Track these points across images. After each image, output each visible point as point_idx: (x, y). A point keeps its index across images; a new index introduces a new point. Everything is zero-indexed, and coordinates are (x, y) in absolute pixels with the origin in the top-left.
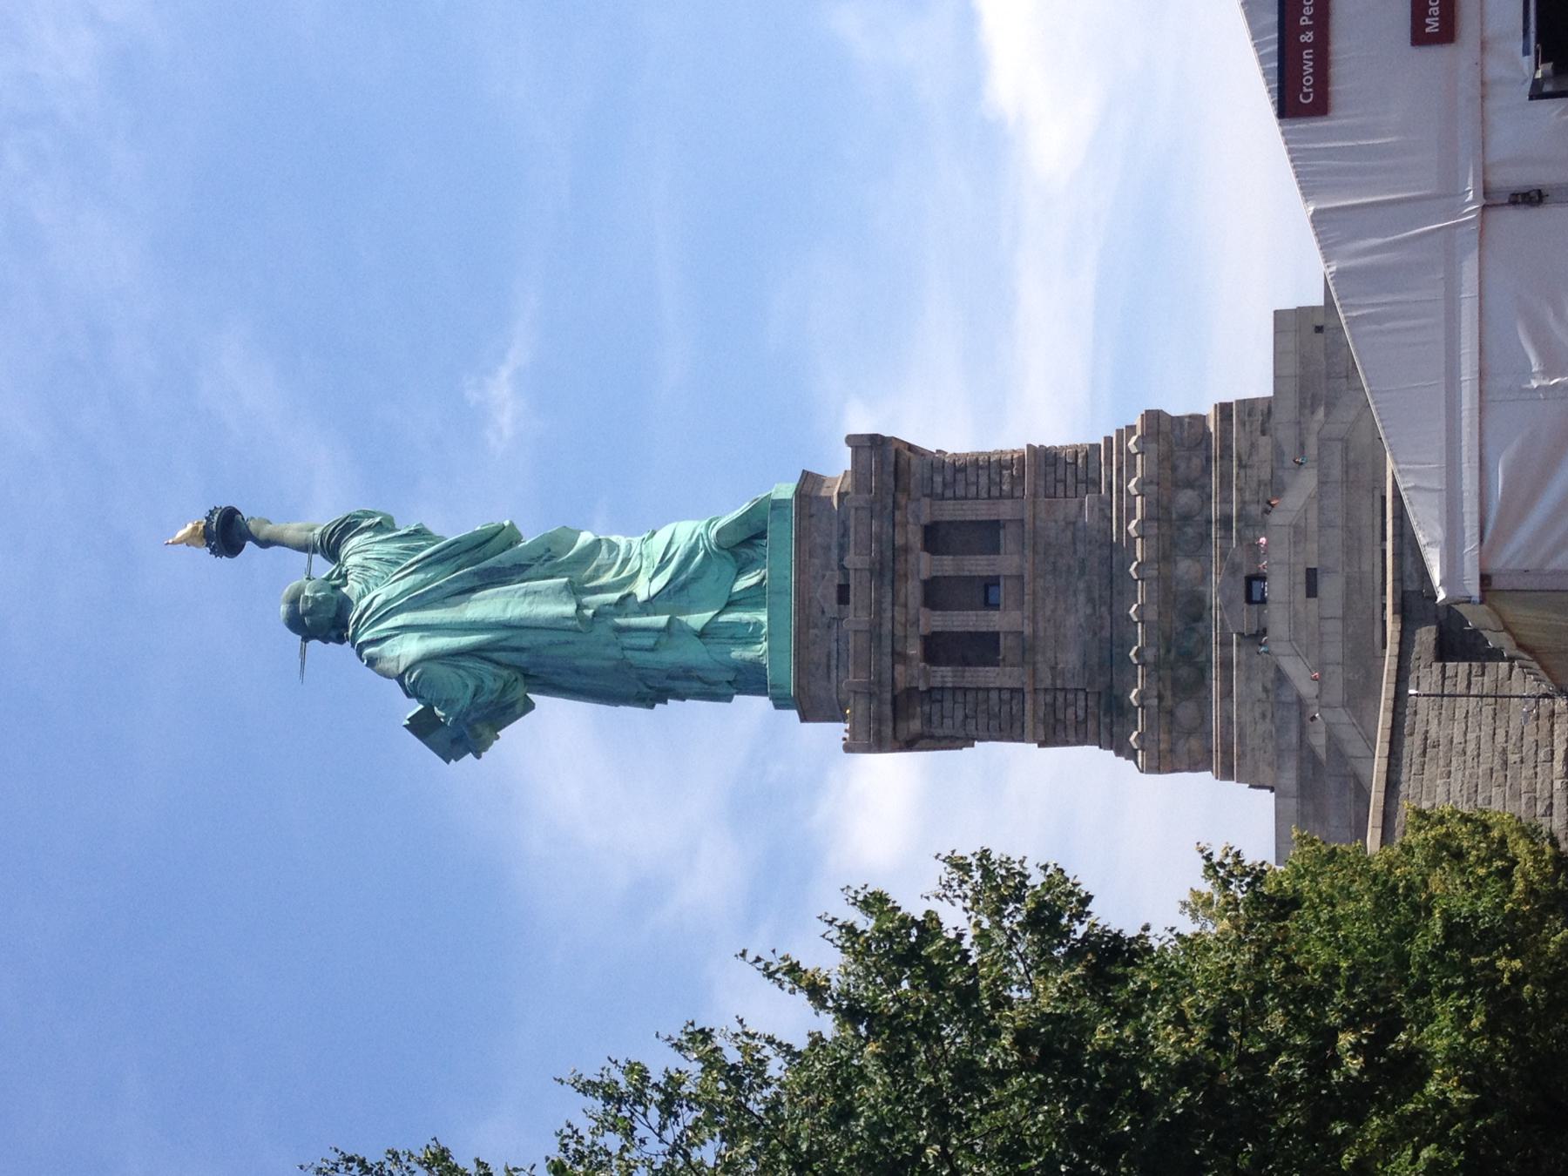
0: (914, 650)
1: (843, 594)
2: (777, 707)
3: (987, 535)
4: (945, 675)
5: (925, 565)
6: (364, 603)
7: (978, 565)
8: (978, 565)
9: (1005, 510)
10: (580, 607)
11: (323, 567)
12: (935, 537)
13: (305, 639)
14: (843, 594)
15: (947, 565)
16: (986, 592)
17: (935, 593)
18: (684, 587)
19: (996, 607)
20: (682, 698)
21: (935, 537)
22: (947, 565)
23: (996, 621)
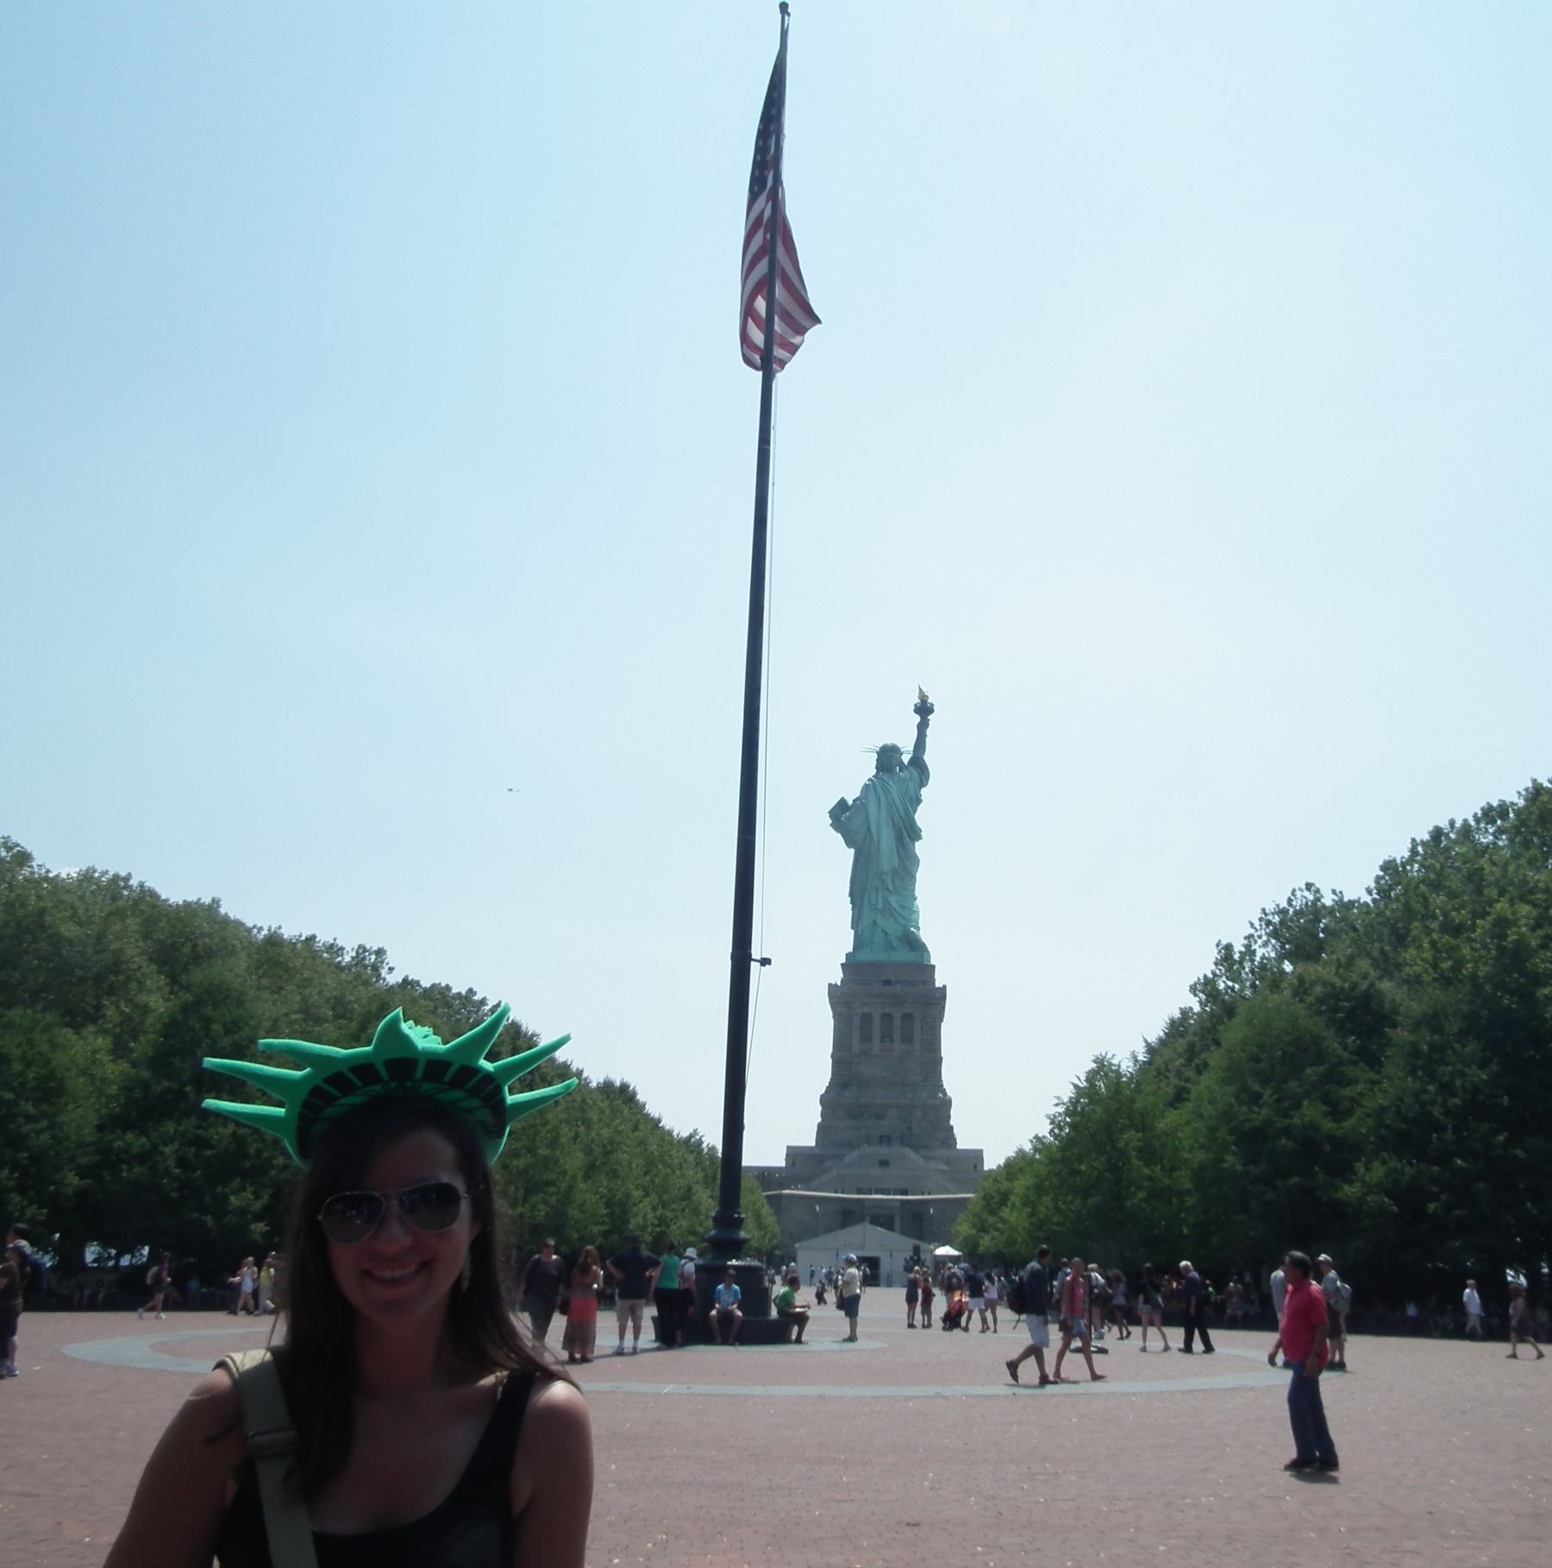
0: (865, 1010)
1: (887, 982)
2: (847, 954)
3: (908, 1039)
4: (856, 1022)
5: (897, 1014)
6: (891, 783)
7: (897, 1034)
8: (897, 1034)
9: (917, 1045)
10: (886, 873)
11: (906, 759)
12: (908, 1018)
13: (877, 753)
14: (887, 982)
15: (897, 1023)
16: (886, 1036)
17: (887, 1017)
18: (893, 916)
19: (882, 1040)
20: (852, 910)
21: (908, 1018)
22: (897, 1023)
23: (876, 1041)
